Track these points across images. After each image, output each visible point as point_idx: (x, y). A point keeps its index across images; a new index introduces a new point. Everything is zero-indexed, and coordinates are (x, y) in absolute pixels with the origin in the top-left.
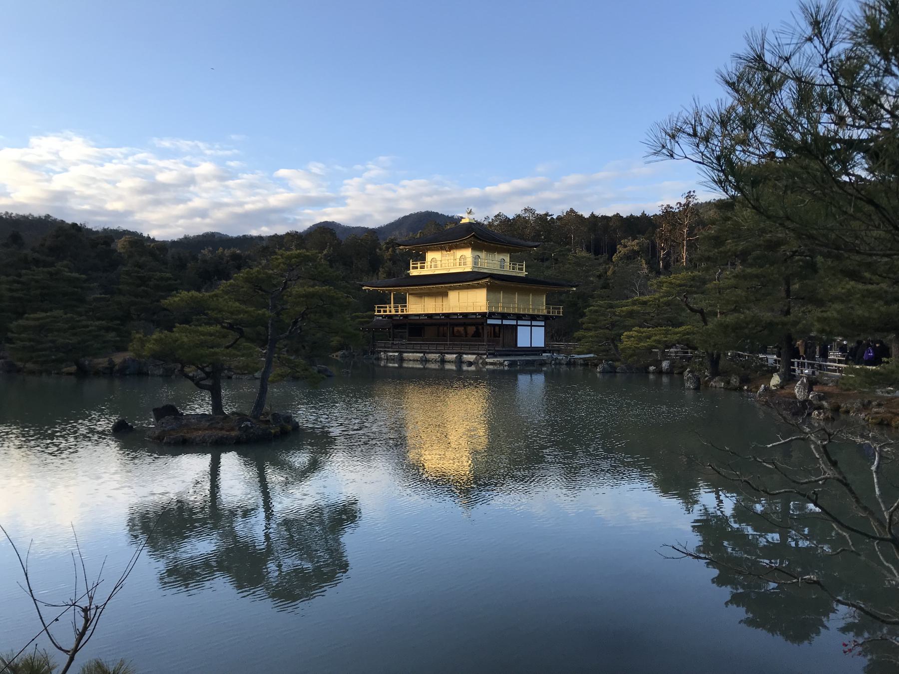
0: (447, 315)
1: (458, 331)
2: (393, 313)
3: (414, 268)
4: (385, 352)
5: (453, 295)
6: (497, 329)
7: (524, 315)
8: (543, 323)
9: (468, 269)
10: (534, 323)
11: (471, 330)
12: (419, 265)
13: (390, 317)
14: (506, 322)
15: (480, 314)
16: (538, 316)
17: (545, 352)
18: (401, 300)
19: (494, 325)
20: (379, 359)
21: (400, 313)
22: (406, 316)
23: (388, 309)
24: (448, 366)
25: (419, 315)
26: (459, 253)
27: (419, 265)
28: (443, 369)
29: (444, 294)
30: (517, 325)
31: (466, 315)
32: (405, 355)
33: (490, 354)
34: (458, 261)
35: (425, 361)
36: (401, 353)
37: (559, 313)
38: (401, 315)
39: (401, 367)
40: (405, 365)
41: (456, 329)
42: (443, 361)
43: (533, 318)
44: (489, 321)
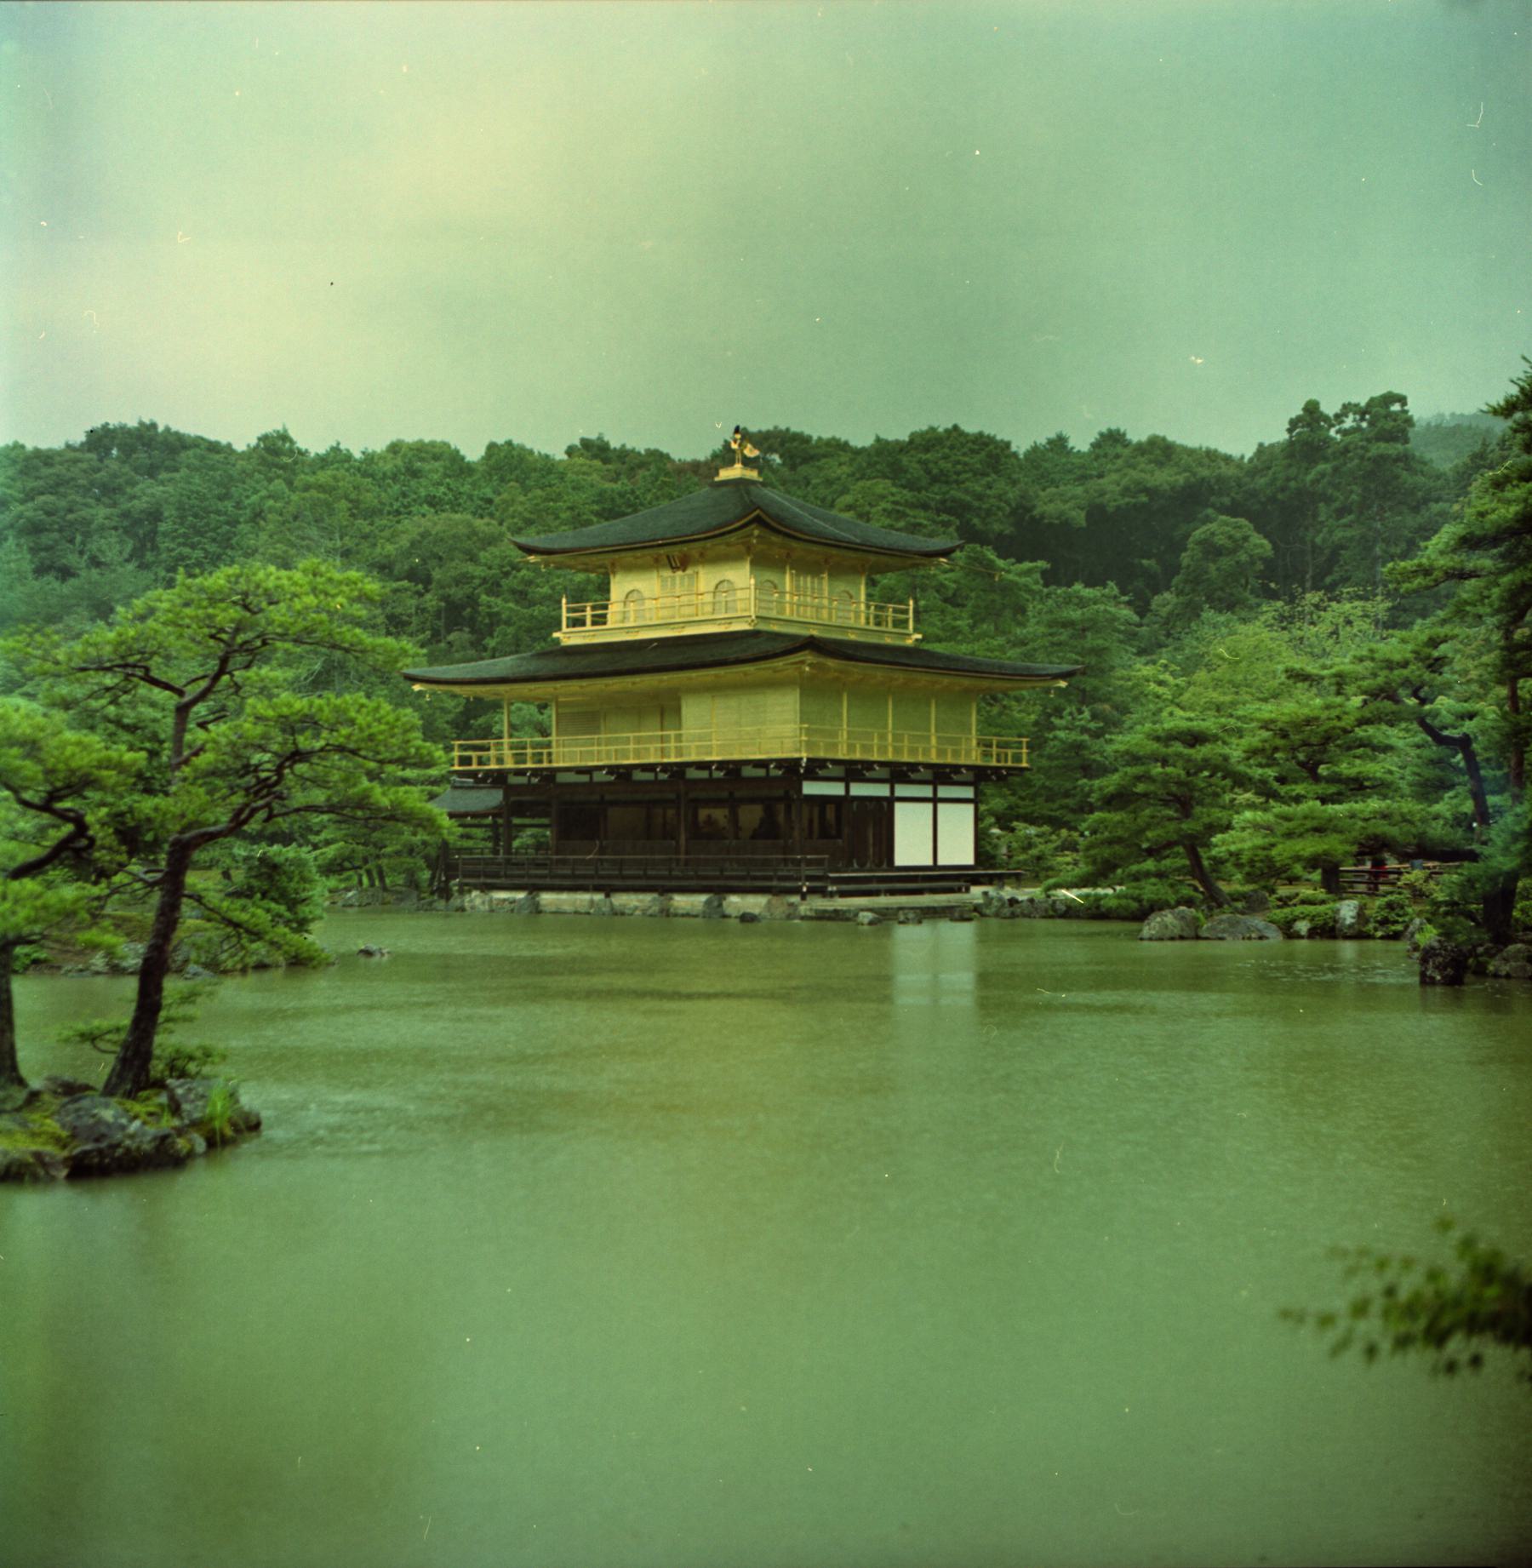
0: (677, 771)
1: (709, 819)
2: (509, 765)
3: (578, 622)
4: (486, 888)
6: (830, 813)
7: (913, 767)
8: (968, 792)
10: (944, 791)
11: (751, 816)
12: (589, 613)
13: (498, 779)
14: (858, 790)
15: (780, 763)
16: (956, 768)
17: (977, 881)
19: (824, 800)
21: (529, 765)
22: (548, 776)
23: (492, 753)
25: (588, 771)
27: (589, 613)
29: (666, 709)
30: (892, 800)
31: (732, 769)
32: (547, 898)
33: (812, 891)
34: (708, 598)
37: (1017, 758)
38: (535, 772)
41: (703, 813)
43: (942, 775)
44: (810, 788)
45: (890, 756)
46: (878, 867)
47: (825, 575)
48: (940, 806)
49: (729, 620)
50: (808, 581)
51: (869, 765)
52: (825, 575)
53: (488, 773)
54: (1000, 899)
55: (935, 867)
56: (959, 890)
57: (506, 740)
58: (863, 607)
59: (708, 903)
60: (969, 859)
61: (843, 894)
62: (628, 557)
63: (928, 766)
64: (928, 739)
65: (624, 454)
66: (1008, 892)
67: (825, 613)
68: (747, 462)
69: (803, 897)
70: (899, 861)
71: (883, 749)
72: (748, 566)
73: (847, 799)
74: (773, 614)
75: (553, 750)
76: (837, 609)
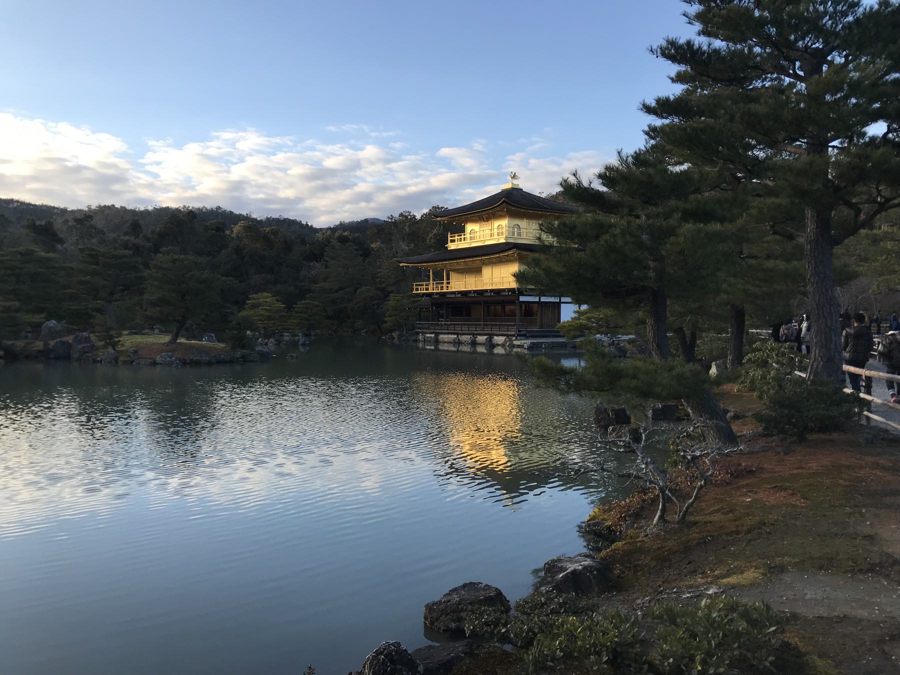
4: (423, 333)
5: (487, 271)
9: (502, 241)
18: (438, 276)
20: (417, 341)
24: (481, 349)
26: (496, 223)
28: (475, 352)
29: (478, 271)
30: (560, 303)
31: (498, 292)
32: (441, 336)
33: (518, 335)
35: (458, 343)
36: (437, 334)
38: (437, 294)
39: (437, 349)
40: (441, 347)
42: (474, 344)
44: (522, 299)
53: (424, 294)
57: (431, 282)
61: (533, 337)
73: (540, 303)
75: (445, 285)
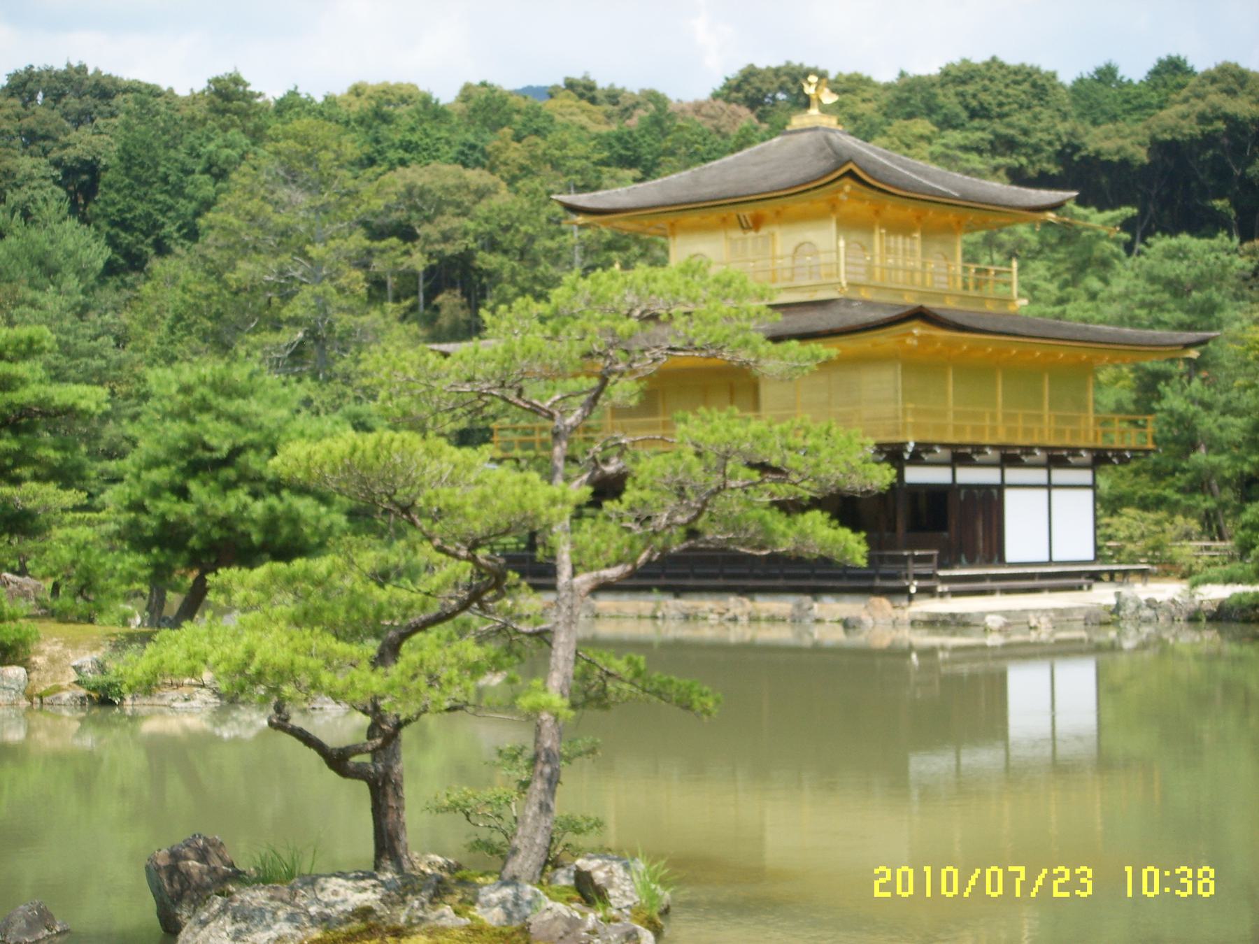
7: (1028, 450)
8: (1085, 476)
10: (1059, 475)
14: (967, 476)
16: (1075, 451)
17: (1096, 577)
30: (1001, 487)
33: (921, 591)
34: (787, 262)
43: (1056, 459)
45: (1002, 438)
46: (989, 562)
47: (917, 235)
48: (1055, 492)
49: (815, 288)
50: (899, 242)
51: (979, 448)
52: (917, 235)
54: (1136, 600)
55: (1051, 562)
56: (1080, 588)
58: (959, 270)
59: (799, 606)
60: (1085, 551)
61: (955, 594)
62: (694, 218)
63: (1043, 448)
64: (1039, 418)
65: (613, 97)
66: (1142, 591)
67: (918, 277)
68: (825, 110)
69: (911, 598)
70: (1010, 556)
71: (994, 430)
72: (833, 226)
74: (861, 279)
76: (933, 273)
